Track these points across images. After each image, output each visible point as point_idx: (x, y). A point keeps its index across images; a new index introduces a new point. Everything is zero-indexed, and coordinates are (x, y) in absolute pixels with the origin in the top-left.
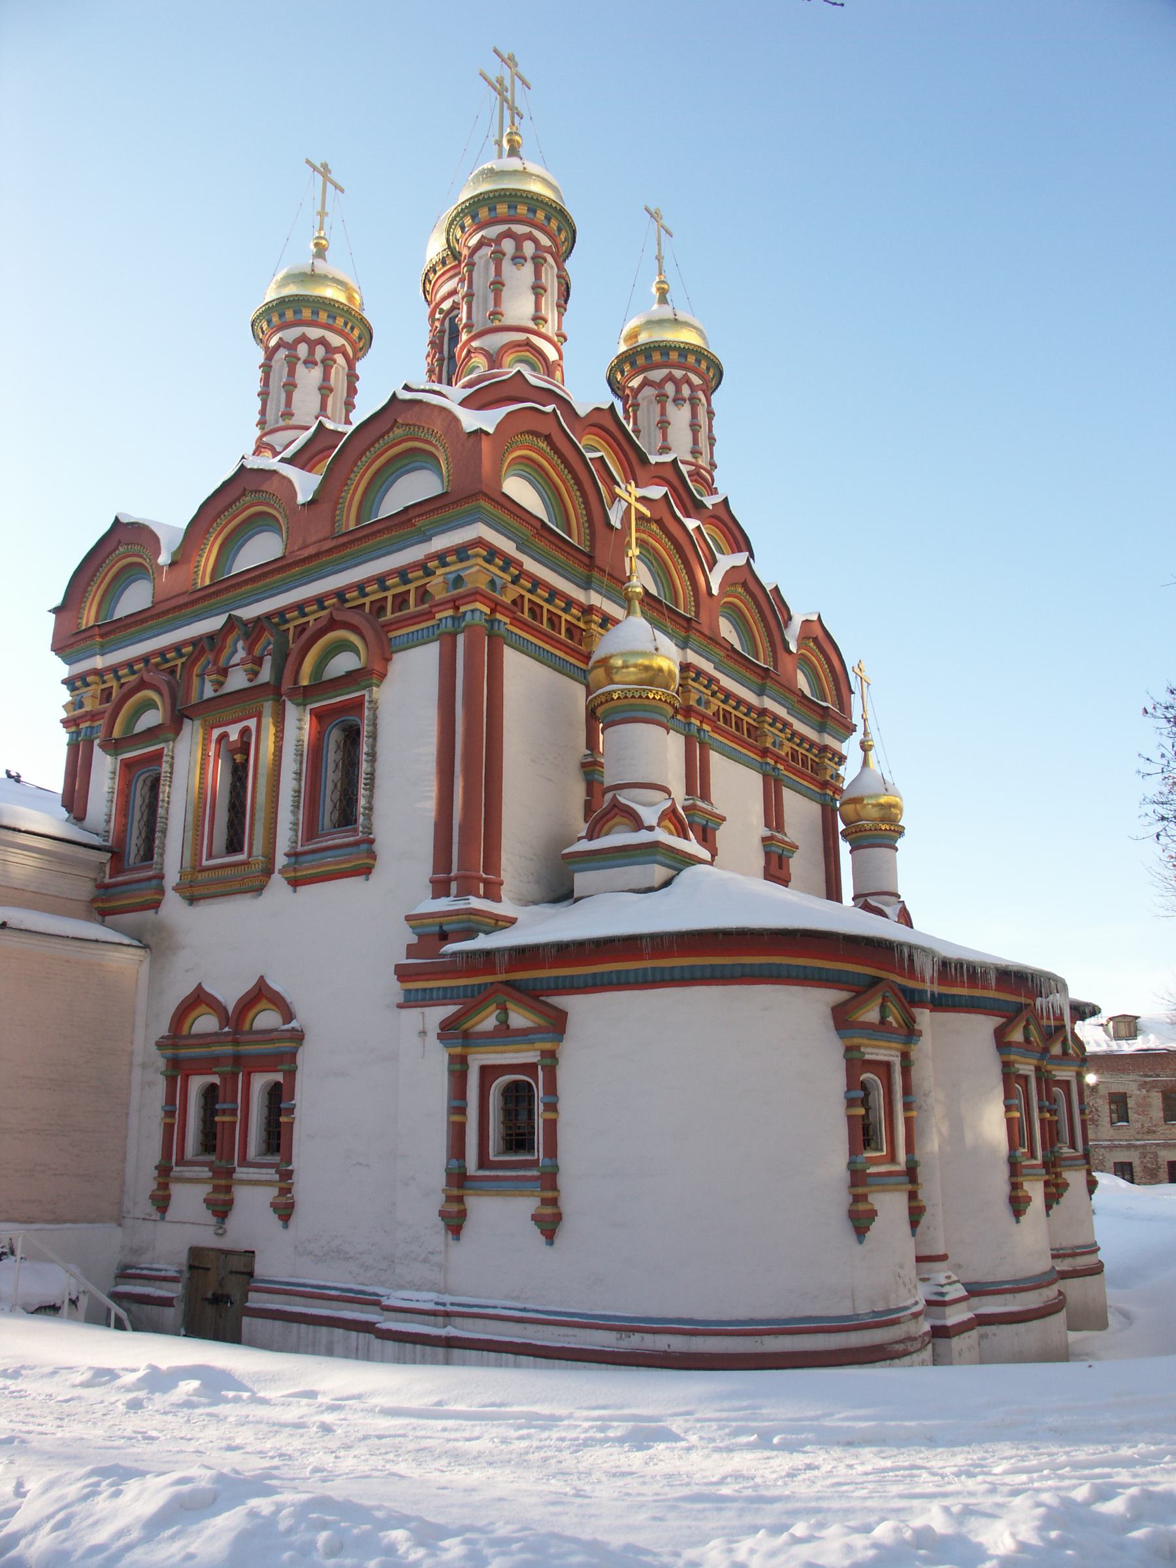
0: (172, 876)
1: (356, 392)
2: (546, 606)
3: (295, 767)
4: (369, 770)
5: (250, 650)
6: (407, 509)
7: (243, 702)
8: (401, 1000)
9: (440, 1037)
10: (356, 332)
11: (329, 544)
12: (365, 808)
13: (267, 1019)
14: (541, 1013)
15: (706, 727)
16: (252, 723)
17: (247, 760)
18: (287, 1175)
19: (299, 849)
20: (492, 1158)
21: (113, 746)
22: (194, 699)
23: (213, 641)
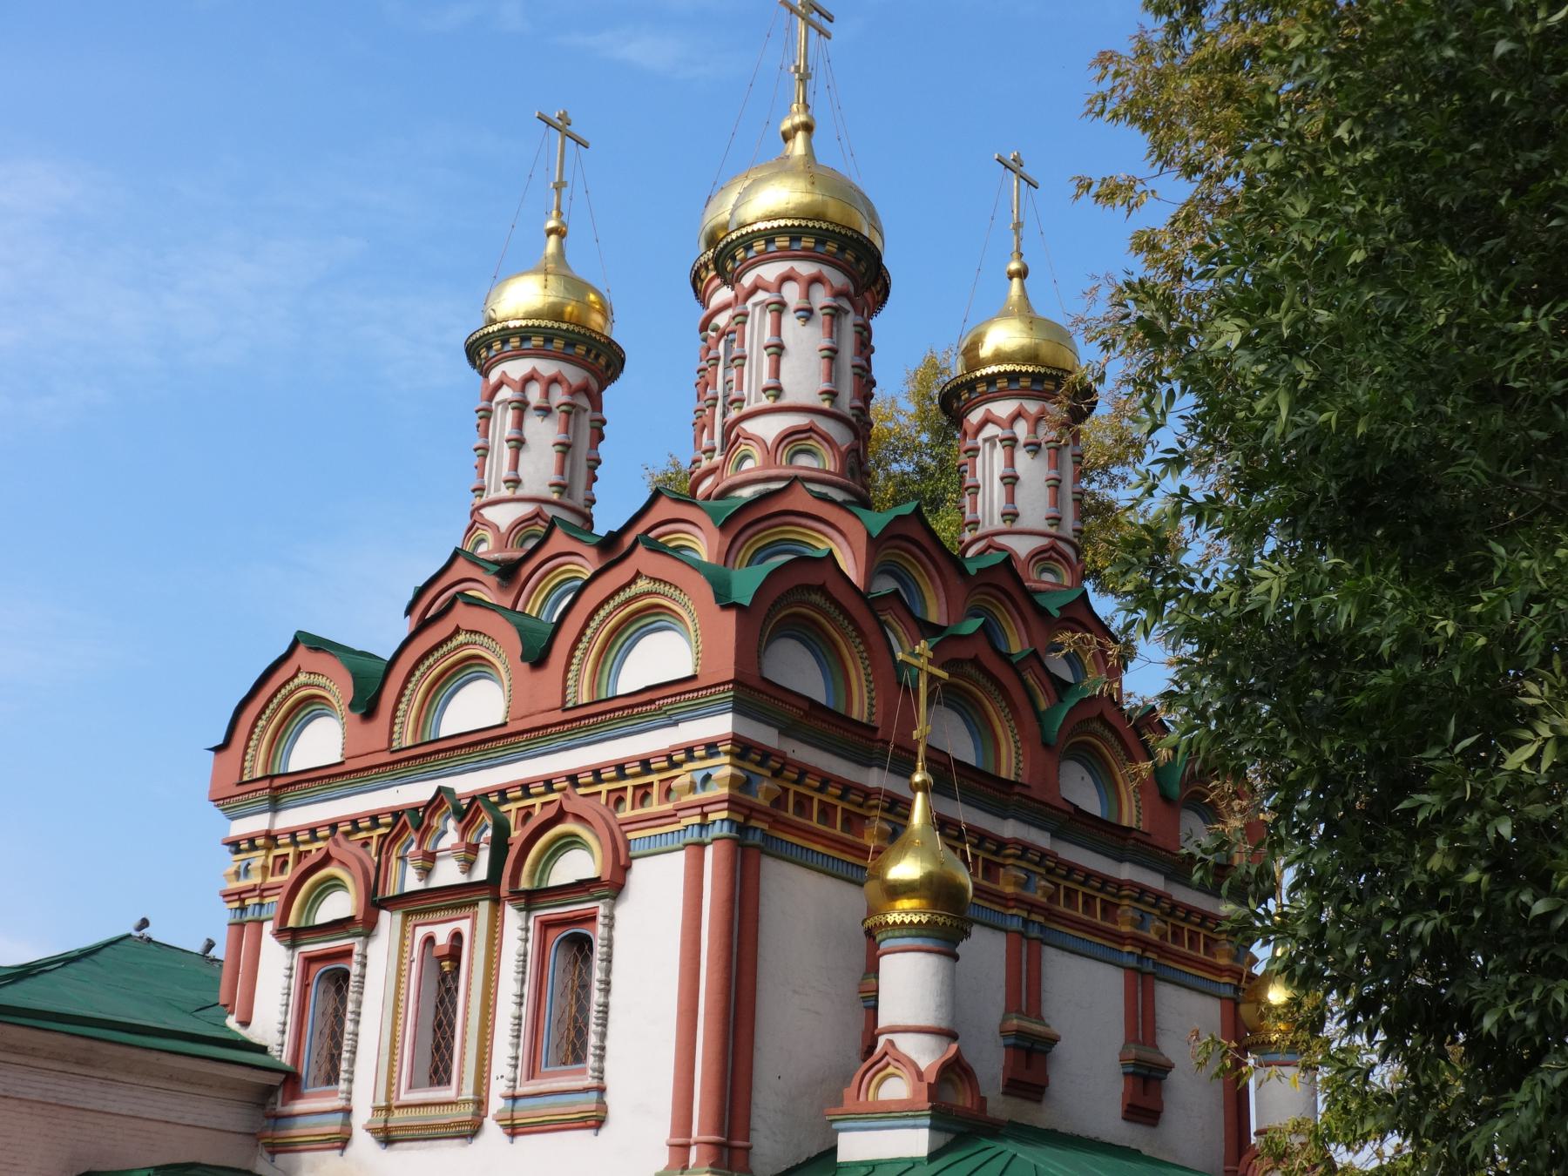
0: (362, 1115)
1: (601, 437)
2: (817, 796)
3: (515, 988)
4: (602, 1000)
5: (463, 833)
7: (457, 898)
10: (602, 361)
11: (559, 716)
12: (596, 1048)
15: (1034, 917)
16: (464, 926)
17: (458, 968)
19: (520, 1090)
21: (292, 936)
22: (392, 890)
23: (417, 820)
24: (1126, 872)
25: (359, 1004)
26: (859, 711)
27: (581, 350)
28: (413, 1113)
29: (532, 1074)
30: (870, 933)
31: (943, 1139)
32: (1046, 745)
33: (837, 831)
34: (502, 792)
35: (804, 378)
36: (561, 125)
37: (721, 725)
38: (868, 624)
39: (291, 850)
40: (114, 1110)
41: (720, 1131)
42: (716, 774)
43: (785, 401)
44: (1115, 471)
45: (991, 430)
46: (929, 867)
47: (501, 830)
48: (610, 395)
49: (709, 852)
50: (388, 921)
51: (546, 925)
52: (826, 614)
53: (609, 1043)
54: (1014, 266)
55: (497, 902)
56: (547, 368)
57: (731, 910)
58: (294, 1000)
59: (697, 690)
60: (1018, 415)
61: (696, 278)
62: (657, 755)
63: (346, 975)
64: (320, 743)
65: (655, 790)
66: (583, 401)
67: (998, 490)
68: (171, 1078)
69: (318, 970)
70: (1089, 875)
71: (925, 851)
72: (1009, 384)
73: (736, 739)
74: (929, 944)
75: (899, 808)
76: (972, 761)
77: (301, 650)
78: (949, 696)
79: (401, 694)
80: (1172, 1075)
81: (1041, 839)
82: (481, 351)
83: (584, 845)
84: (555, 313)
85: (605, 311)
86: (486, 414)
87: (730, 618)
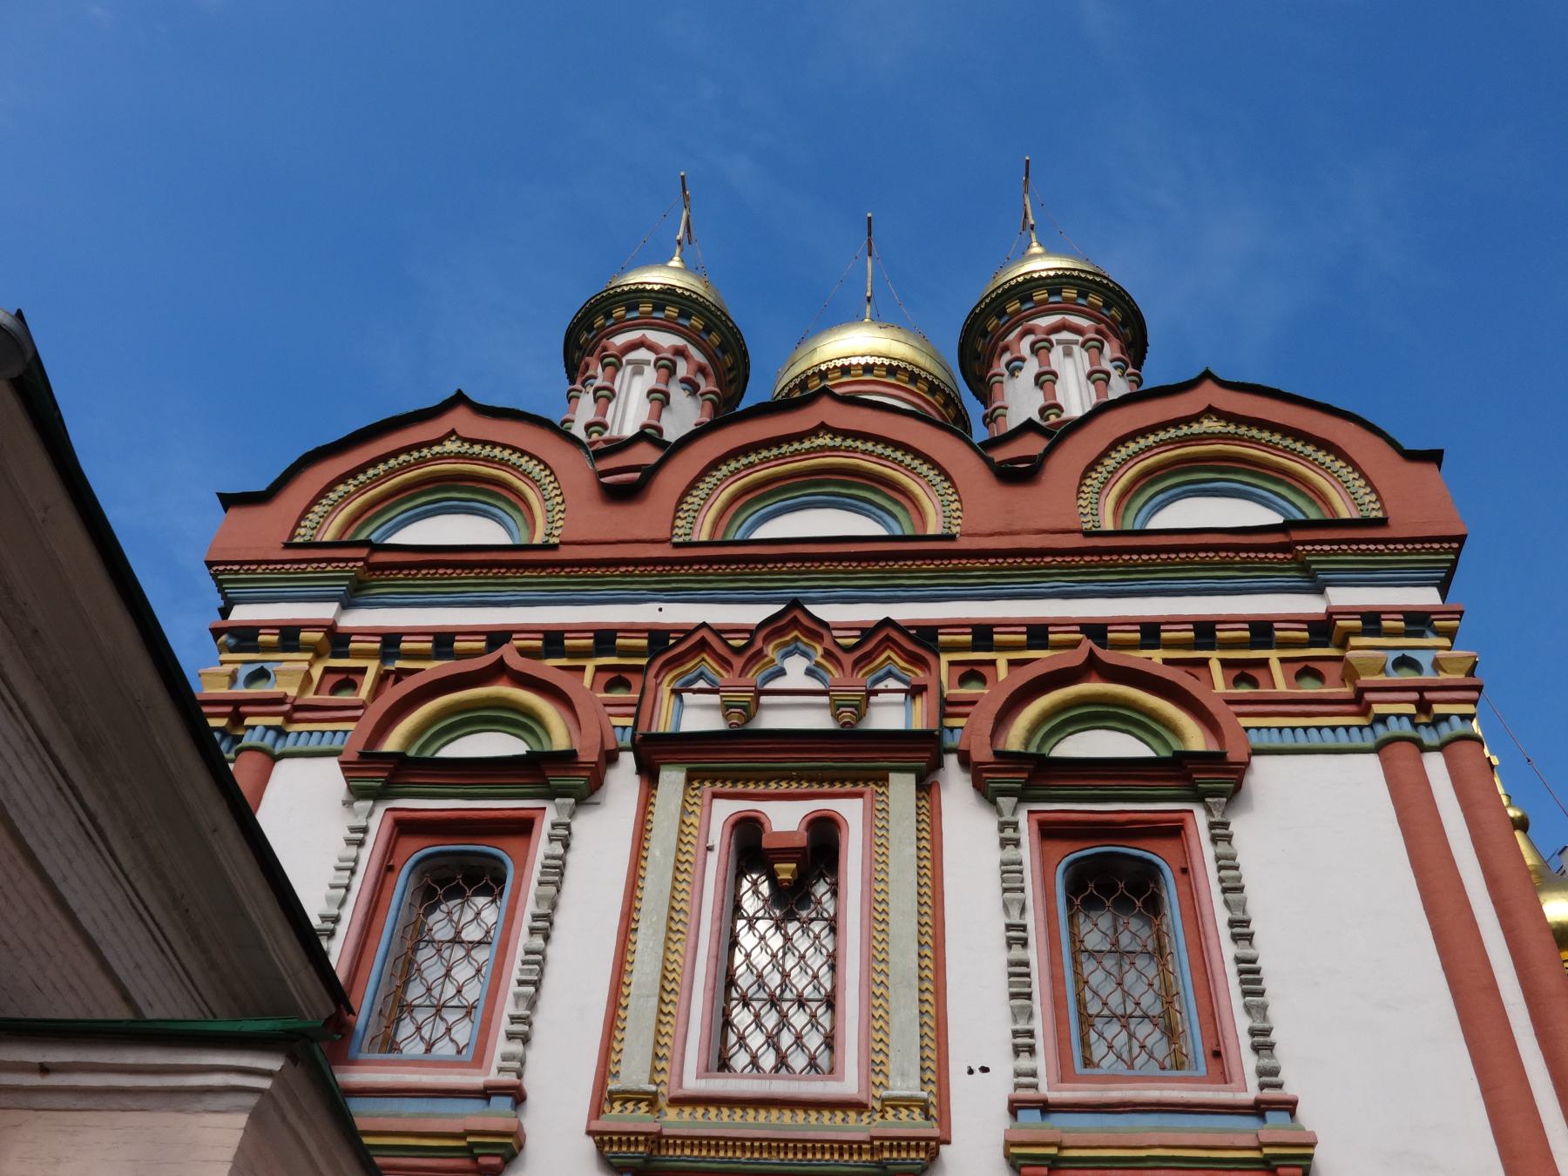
16: (850, 811)
39: (373, 666)
40: (74, 904)
59: (1385, 541)
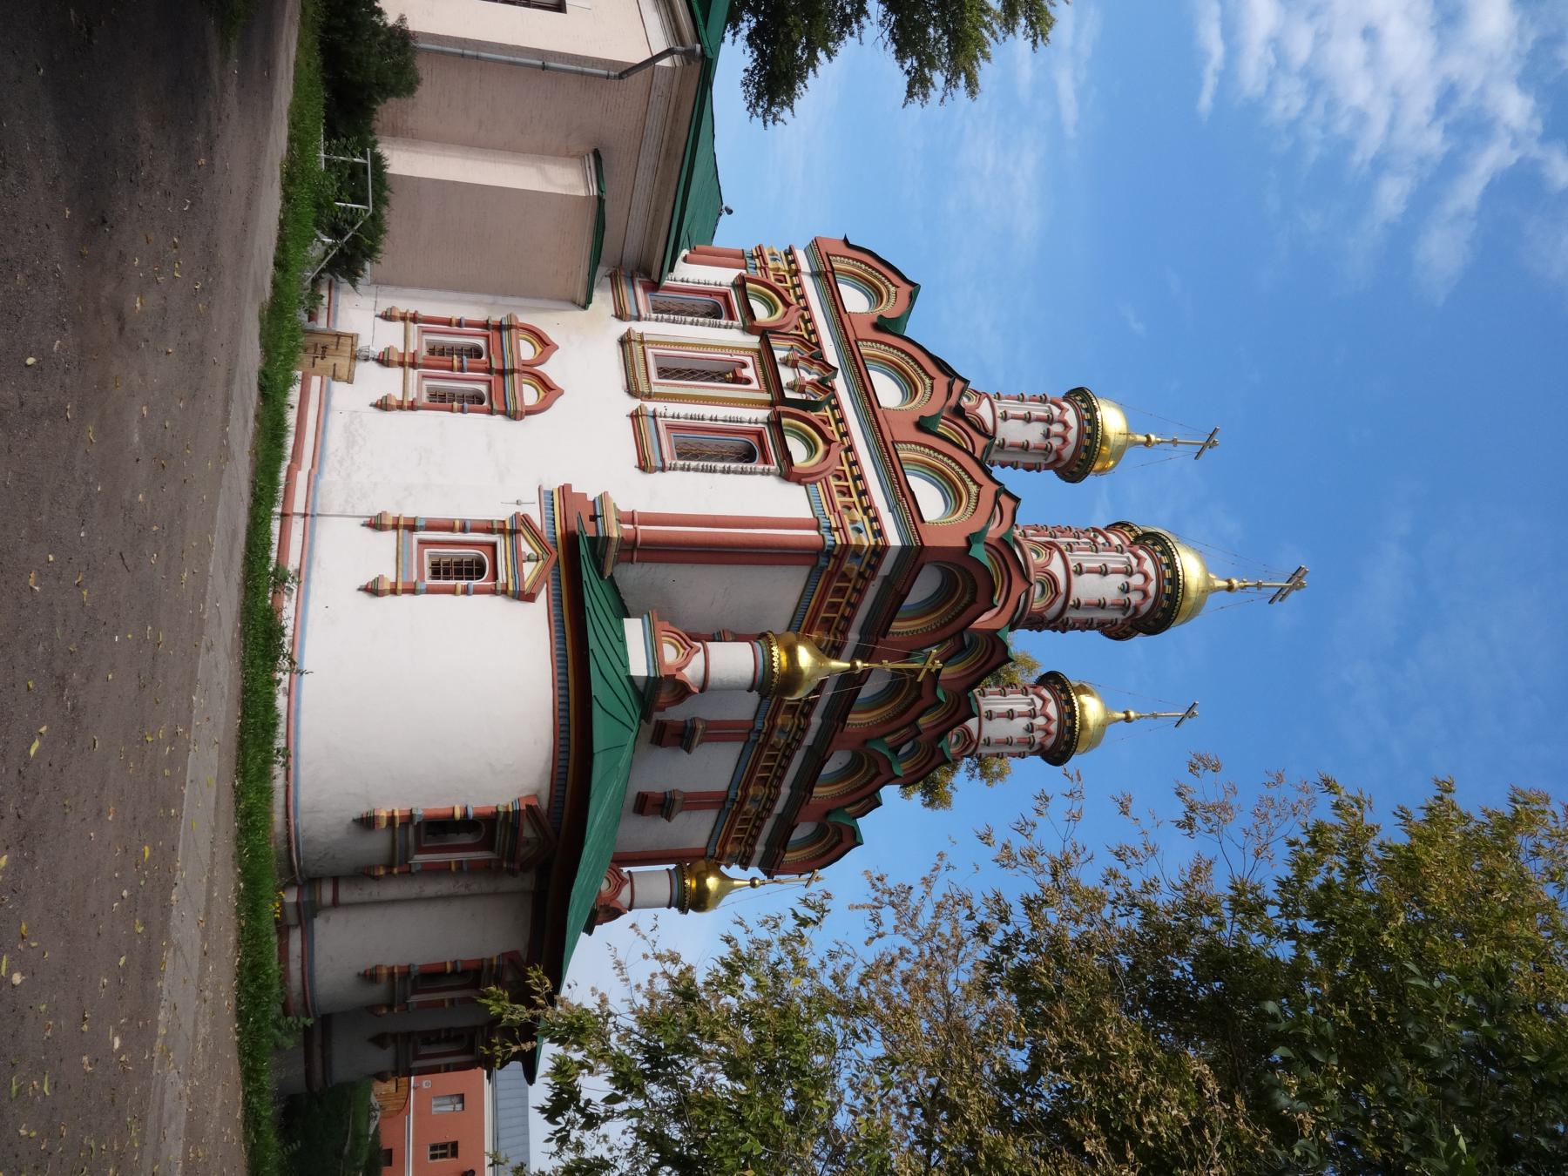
0: (638, 327)
1: (1028, 470)
3: (720, 416)
5: (811, 383)
6: (912, 494)
7: (771, 380)
8: (546, 488)
9: (516, 515)
11: (889, 439)
13: (530, 395)
14: (534, 583)
16: (755, 385)
18: (413, 407)
20: (426, 551)
21: (740, 285)
22: (774, 343)
23: (817, 358)
24: (785, 790)
25: (703, 325)
26: (897, 626)
27: (1083, 456)
28: (641, 357)
29: (669, 427)
30: (763, 635)
31: (640, 684)
32: (865, 742)
33: (822, 615)
34: (837, 406)
35: (1088, 588)
36: (1210, 443)
37: (894, 539)
38: (949, 631)
41: (644, 543)
42: (863, 535)
43: (1074, 578)
44: (978, 770)
45: (1039, 703)
46: (807, 672)
47: (815, 406)
48: (1050, 474)
49: (814, 533)
50: (754, 341)
51: (759, 434)
52: (957, 603)
53: (691, 473)
54: (1132, 714)
55: (771, 404)
56: (1072, 436)
57: (780, 547)
58: (701, 287)
60: (1049, 719)
61: (1123, 525)
62: (871, 500)
63: (719, 317)
64: (855, 300)
65: (847, 499)
66: (1052, 458)
67: (1004, 708)
68: (657, 210)
69: (720, 301)
70: (785, 769)
71: (816, 668)
72: (1068, 712)
73: (886, 548)
74: (760, 673)
75: (835, 651)
76: (860, 696)
77: (909, 288)
78: (899, 682)
79: (890, 346)
80: (663, 820)
81: (809, 740)
82: (1080, 397)
83: (810, 457)
84: (1105, 440)
85: (1103, 470)
86: (1043, 400)
87: (960, 542)
